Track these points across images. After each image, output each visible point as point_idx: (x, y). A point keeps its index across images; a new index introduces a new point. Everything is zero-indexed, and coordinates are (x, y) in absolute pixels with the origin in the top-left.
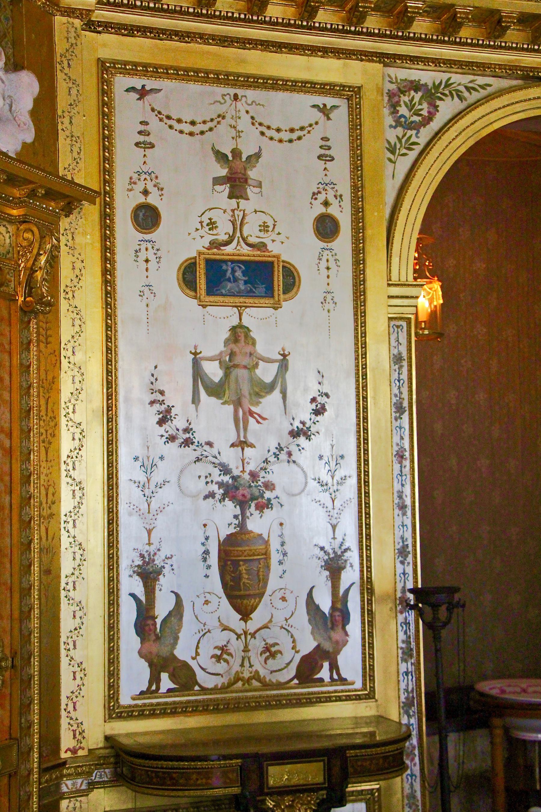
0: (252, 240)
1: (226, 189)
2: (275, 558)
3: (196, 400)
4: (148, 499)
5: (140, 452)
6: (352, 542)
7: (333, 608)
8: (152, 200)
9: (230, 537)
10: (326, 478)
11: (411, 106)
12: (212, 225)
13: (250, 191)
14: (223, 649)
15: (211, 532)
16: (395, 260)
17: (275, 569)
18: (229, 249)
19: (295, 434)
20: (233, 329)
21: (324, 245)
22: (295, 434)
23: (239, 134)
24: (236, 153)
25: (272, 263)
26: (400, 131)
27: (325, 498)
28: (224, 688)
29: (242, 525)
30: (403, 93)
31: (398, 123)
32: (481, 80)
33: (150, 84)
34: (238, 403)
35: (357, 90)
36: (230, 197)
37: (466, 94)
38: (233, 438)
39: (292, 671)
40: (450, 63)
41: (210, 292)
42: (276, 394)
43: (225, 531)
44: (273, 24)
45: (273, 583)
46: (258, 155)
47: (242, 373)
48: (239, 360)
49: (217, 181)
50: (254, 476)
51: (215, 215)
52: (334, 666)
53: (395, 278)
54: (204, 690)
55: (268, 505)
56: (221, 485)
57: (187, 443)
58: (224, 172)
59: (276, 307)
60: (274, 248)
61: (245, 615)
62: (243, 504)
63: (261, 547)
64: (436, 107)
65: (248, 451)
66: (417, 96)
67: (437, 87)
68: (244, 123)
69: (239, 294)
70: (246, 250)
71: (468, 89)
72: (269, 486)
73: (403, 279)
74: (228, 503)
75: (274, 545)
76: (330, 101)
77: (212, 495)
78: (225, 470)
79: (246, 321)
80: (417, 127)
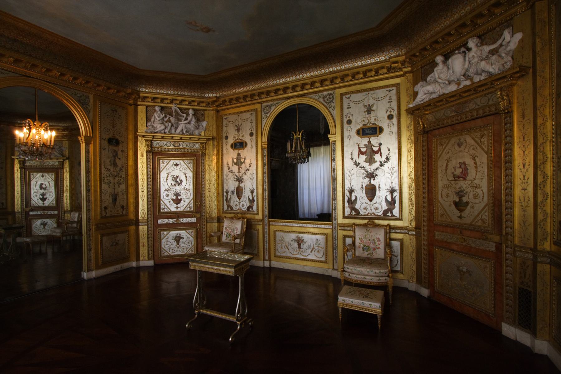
0: (241, 139)
1: (237, 131)
2: (244, 190)
3: (233, 166)
4: (227, 181)
5: (226, 174)
6: (255, 188)
7: (252, 199)
8: (227, 135)
9: (238, 187)
10: (251, 177)
11: (267, 110)
12: (235, 137)
13: (240, 131)
14: (236, 204)
15: (235, 186)
16: (263, 138)
17: (244, 192)
18: (237, 141)
19: (246, 170)
20: (238, 154)
21: (250, 137)
22: (246, 170)
23: (239, 121)
24: (238, 125)
25: (243, 142)
26: (265, 115)
27: (251, 181)
28: (237, 211)
29: (239, 185)
30: (265, 107)
31: (265, 113)
32: (279, 101)
33: (227, 117)
34: (239, 166)
35: (257, 109)
36: (238, 132)
37: (276, 105)
38: (238, 171)
39: (246, 209)
40: (271, 100)
41: (235, 148)
42: (244, 164)
43: (237, 186)
44: (241, 103)
45: (243, 195)
46: (241, 125)
47: (239, 160)
48: (239, 159)
49: (236, 130)
50: (241, 177)
51: (235, 136)
52: (252, 209)
53: (263, 141)
54: (234, 210)
55: (243, 182)
56: (236, 179)
57: (232, 172)
58: (236, 128)
59: (244, 149)
60: (244, 139)
61: (240, 199)
62: (239, 182)
63: (241, 189)
64: (271, 109)
65: (240, 173)
66: (268, 108)
67: (271, 105)
68: (240, 120)
69: (239, 148)
70: (240, 140)
71: (277, 104)
72: (243, 179)
73: (265, 141)
74: (237, 182)
75: (244, 189)
76: (252, 113)
77: (235, 180)
78: (237, 176)
79: (240, 152)
80: (267, 113)
